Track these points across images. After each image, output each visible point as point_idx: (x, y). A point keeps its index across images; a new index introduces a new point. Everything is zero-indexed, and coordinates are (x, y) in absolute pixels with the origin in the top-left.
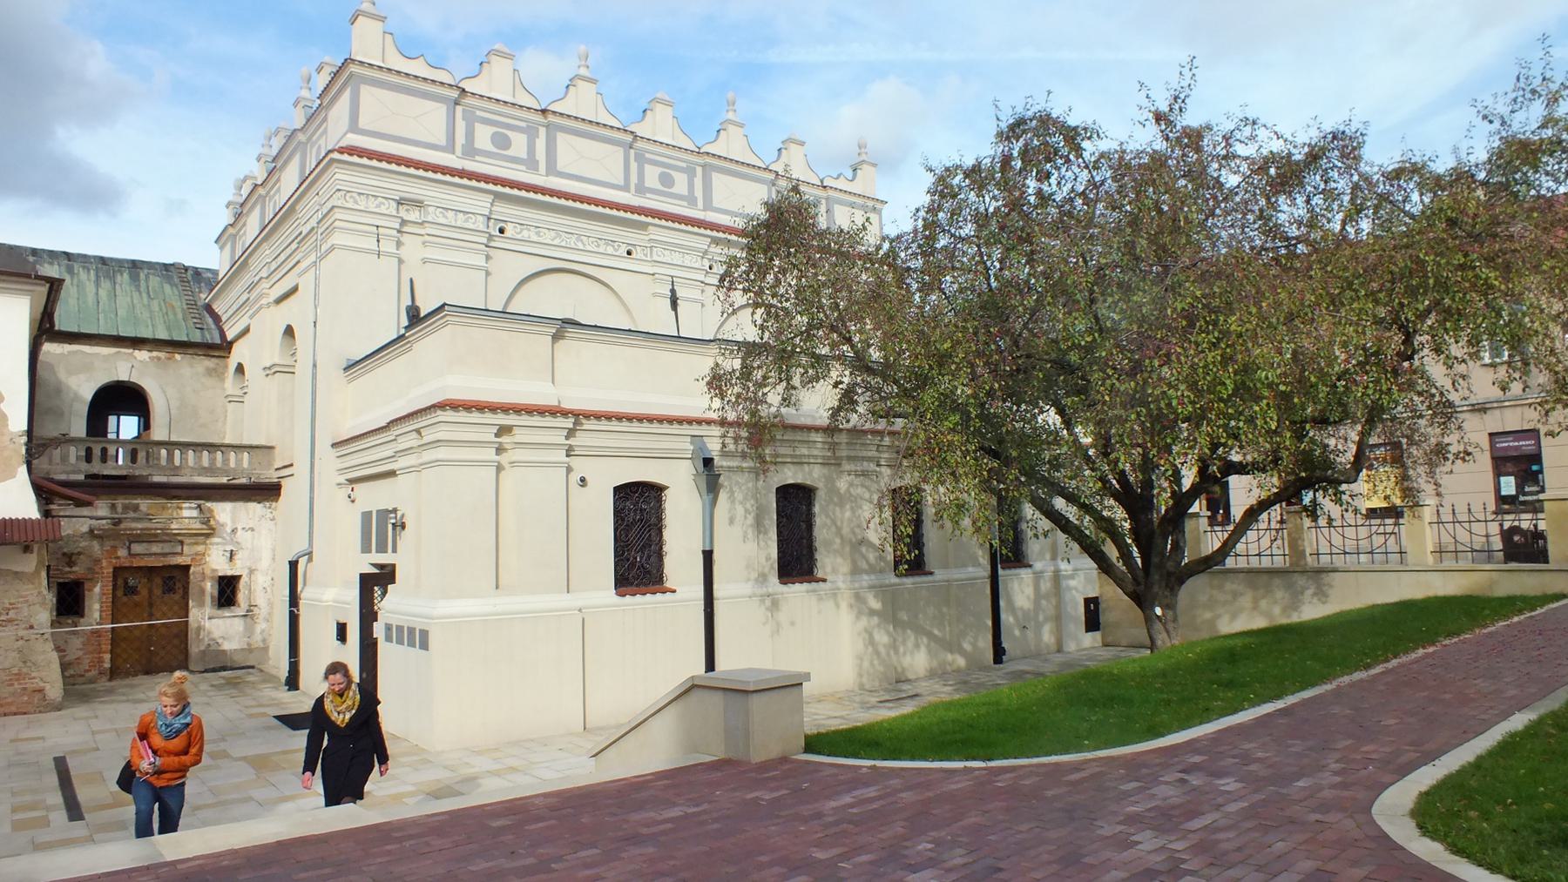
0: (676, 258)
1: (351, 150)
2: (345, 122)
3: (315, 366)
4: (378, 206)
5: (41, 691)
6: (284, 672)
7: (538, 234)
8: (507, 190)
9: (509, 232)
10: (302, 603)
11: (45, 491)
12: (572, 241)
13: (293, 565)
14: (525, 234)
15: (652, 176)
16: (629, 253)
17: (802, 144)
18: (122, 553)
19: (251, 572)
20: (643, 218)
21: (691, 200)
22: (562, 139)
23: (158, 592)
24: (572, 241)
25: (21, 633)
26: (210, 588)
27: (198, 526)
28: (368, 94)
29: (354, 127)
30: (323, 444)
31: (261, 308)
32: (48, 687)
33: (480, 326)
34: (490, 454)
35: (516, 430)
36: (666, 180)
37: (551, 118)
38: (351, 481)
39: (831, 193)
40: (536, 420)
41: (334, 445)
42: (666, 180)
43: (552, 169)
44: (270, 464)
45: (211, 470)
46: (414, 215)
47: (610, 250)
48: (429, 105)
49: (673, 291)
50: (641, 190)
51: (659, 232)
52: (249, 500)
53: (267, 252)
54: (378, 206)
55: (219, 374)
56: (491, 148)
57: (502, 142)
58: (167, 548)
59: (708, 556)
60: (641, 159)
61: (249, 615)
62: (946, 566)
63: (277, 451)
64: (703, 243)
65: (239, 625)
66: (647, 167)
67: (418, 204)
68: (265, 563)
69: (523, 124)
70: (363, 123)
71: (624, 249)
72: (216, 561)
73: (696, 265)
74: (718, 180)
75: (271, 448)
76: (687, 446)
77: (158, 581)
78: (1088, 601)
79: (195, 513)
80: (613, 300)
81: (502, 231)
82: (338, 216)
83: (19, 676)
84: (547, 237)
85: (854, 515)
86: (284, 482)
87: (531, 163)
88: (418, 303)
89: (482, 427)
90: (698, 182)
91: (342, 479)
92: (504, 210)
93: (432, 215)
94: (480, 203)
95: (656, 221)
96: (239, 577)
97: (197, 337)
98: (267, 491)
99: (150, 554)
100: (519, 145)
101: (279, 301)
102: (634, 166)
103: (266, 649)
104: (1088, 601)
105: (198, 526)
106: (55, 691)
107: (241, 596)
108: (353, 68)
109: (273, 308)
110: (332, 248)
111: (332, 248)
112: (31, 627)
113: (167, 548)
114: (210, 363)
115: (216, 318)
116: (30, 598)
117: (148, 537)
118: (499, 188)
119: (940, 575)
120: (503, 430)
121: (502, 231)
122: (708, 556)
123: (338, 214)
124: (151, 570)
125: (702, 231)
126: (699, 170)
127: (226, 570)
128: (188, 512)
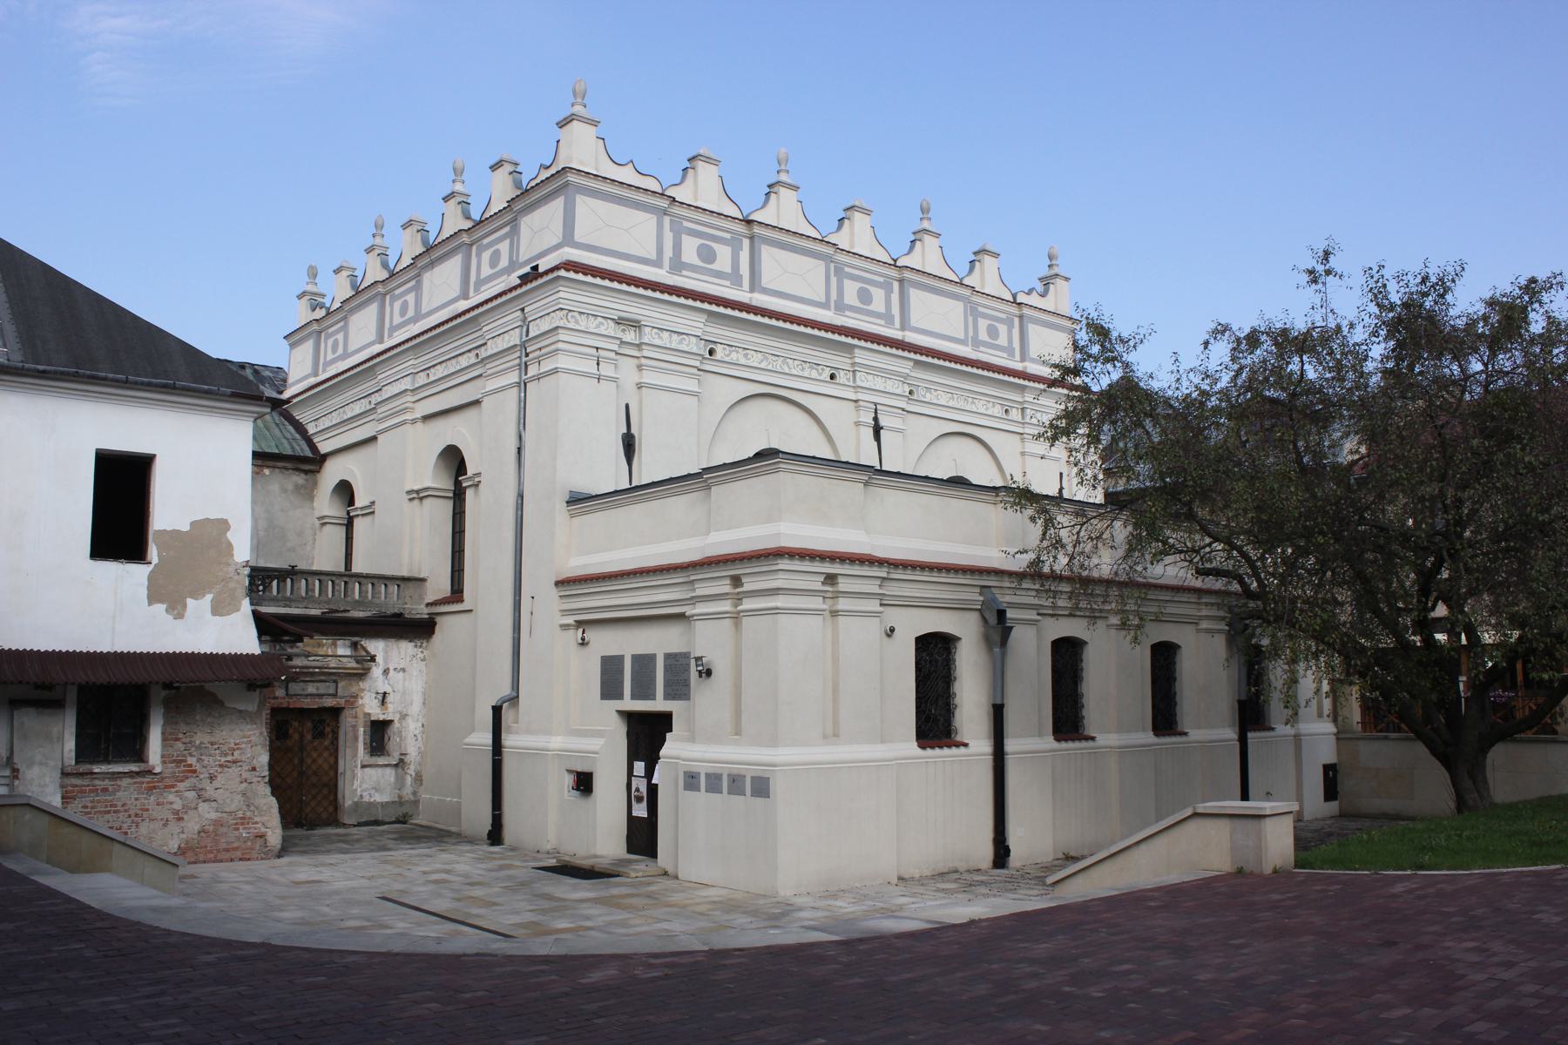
0: (879, 383)
1: (570, 266)
2: (554, 235)
3: (521, 496)
4: (598, 327)
5: (262, 836)
6: (486, 824)
8: (721, 310)
9: (719, 354)
11: (264, 625)
12: (778, 365)
13: (497, 711)
14: (734, 357)
15: (851, 290)
17: (996, 255)
19: (404, 716)
20: (849, 340)
21: (888, 318)
24: (778, 365)
25: (246, 775)
27: (354, 665)
28: (583, 204)
29: (568, 239)
30: (539, 583)
31: (403, 423)
32: (269, 833)
35: (840, 580)
36: (865, 296)
37: (757, 230)
38: (579, 623)
39: (1026, 311)
40: (909, 575)
41: (558, 583)
42: (865, 296)
44: (421, 598)
45: (360, 604)
46: (630, 336)
47: (814, 374)
49: (876, 419)
50: (841, 307)
51: (865, 355)
53: (410, 363)
54: (598, 327)
56: (697, 262)
57: (707, 255)
60: (839, 272)
61: (401, 764)
63: (428, 584)
64: (905, 367)
65: (390, 774)
66: (847, 282)
67: (636, 325)
68: (416, 708)
69: (728, 236)
70: (579, 236)
71: (828, 372)
72: (370, 706)
73: (898, 391)
74: (915, 295)
75: (423, 580)
76: (975, 596)
78: (1327, 768)
79: (348, 652)
80: (815, 428)
81: (711, 352)
82: (562, 337)
83: (244, 821)
84: (755, 359)
85: (1114, 672)
86: (438, 619)
88: (634, 431)
89: (808, 576)
90: (895, 297)
91: (570, 620)
93: (649, 336)
94: (693, 322)
95: (862, 343)
96: (391, 722)
98: (421, 629)
99: (311, 694)
100: (723, 260)
102: (834, 280)
103: (416, 803)
104: (1327, 768)
105: (354, 665)
106: (275, 836)
107: (393, 744)
108: (571, 178)
109: (419, 425)
110: (555, 371)
111: (555, 371)
112: (254, 769)
113: (323, 688)
114: (299, 479)
115: (300, 428)
117: (305, 675)
118: (714, 308)
120: (831, 579)
121: (711, 352)
123: (563, 336)
125: (906, 354)
127: (377, 713)
128: (343, 649)
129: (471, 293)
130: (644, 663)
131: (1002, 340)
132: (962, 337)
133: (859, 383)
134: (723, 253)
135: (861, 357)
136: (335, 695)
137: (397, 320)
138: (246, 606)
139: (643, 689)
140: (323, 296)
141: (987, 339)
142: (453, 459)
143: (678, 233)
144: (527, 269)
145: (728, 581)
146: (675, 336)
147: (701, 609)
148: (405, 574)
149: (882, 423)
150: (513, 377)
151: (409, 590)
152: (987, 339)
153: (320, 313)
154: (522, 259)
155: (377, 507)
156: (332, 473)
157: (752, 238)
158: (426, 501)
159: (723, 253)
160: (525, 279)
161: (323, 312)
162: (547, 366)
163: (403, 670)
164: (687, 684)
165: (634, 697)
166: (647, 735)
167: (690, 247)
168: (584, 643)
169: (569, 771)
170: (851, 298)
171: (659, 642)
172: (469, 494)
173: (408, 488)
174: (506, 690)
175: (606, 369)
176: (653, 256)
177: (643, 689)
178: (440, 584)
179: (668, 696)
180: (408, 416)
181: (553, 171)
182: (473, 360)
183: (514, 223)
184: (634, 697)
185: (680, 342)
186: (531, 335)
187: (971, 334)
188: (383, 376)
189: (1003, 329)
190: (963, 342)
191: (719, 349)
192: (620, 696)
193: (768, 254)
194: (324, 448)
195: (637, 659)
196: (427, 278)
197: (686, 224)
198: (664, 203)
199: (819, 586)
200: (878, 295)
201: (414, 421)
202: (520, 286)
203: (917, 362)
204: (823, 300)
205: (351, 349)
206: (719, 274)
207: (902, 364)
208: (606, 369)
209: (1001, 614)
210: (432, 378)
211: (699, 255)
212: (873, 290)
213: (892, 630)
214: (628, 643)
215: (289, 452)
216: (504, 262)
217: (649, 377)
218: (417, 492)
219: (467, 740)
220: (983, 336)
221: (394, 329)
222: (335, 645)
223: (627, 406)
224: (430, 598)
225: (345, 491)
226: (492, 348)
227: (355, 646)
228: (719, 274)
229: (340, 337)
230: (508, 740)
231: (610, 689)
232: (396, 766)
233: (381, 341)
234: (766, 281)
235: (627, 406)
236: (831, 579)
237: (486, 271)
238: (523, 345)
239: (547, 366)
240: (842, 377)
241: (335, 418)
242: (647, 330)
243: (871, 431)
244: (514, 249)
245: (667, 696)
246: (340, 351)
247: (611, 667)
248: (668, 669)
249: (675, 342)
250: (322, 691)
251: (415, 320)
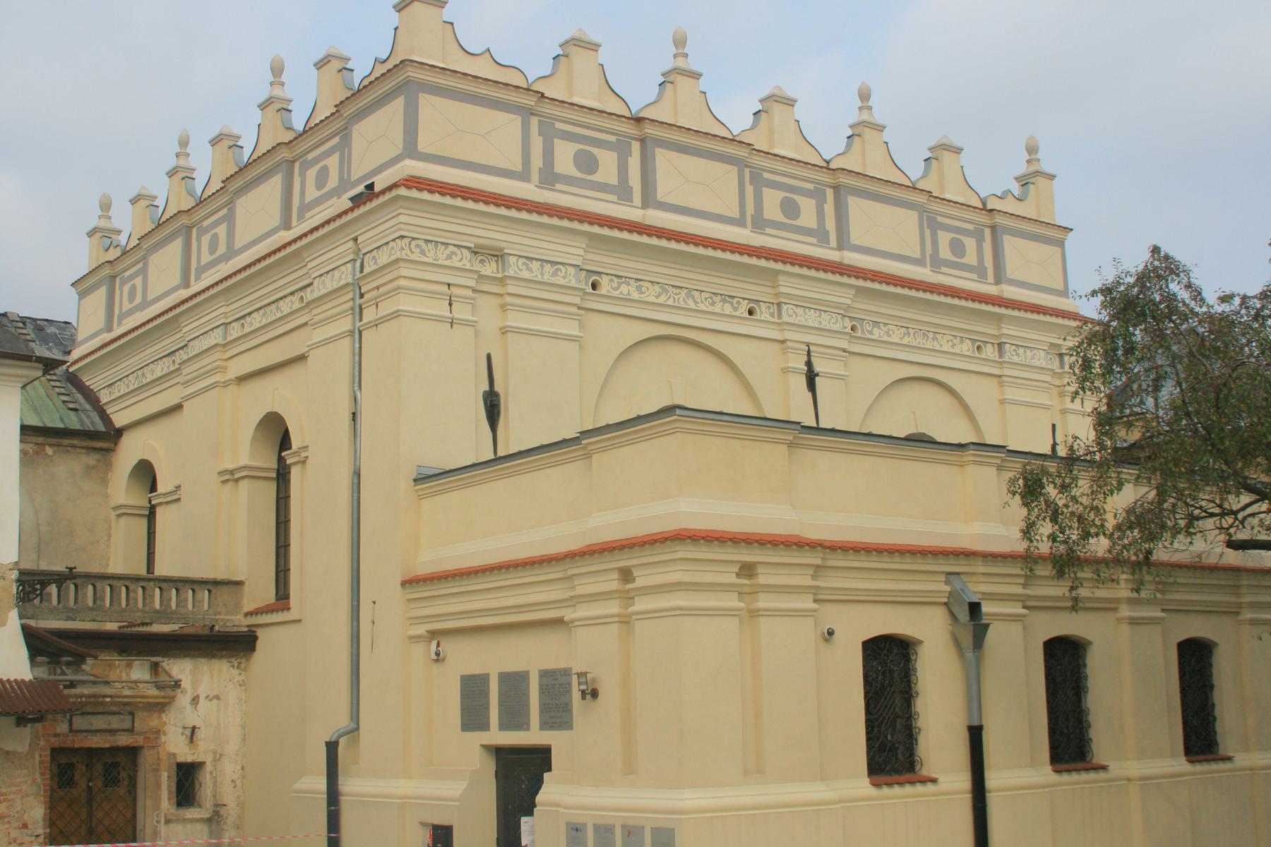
1: (413, 182)
2: (395, 144)
3: (357, 474)
7: (639, 288)
8: (606, 231)
9: (605, 288)
10: (343, 800)
11: (39, 644)
13: (332, 748)
15: (772, 202)
16: (751, 312)
18: (63, 727)
20: (771, 265)
21: (820, 235)
22: (853, 203)
23: (99, 783)
26: (166, 781)
28: (428, 104)
29: (411, 149)
33: (704, 433)
35: (760, 570)
36: (790, 208)
37: (649, 130)
38: (433, 634)
42: (790, 208)
43: (649, 200)
44: (238, 606)
45: (164, 615)
46: (490, 269)
48: (501, 117)
49: (809, 364)
50: (760, 223)
51: (792, 284)
52: (214, 657)
53: (220, 311)
55: (103, 471)
56: (574, 172)
57: (587, 163)
58: (115, 722)
59: (976, 735)
60: (757, 179)
62: (1247, 749)
63: (246, 588)
64: (843, 297)
66: (766, 191)
67: (499, 256)
68: (232, 747)
70: (424, 145)
71: (744, 306)
72: (176, 746)
73: (837, 327)
75: (239, 584)
77: (99, 767)
82: (404, 272)
84: (651, 294)
86: (260, 633)
87: (623, 192)
88: (498, 388)
89: (719, 567)
90: (829, 209)
91: (421, 630)
92: (602, 260)
93: (514, 267)
94: (570, 250)
95: (788, 268)
97: (73, 422)
98: (238, 644)
99: (97, 733)
101: (243, 379)
102: (749, 190)
108: (412, 73)
110: (397, 314)
111: (397, 314)
112: (25, 826)
113: (115, 722)
114: (91, 459)
115: (91, 397)
116: (24, 787)
117: (95, 707)
118: (596, 229)
119: (1241, 759)
121: (594, 286)
122: (976, 735)
124: (91, 753)
125: (845, 280)
126: (830, 193)
127: (185, 754)
128: (139, 671)
129: (294, 222)
130: (514, 683)
131: (970, 258)
132: (917, 255)
133: (786, 318)
134: (608, 162)
135: (788, 286)
136: (131, 731)
137: (206, 258)
138: (14, 620)
139: (514, 717)
140: (119, 232)
141: (950, 257)
142: (277, 432)
143: (549, 134)
144: (360, 188)
145: (615, 575)
146: (547, 267)
147: (582, 612)
148: (220, 576)
149: (818, 367)
150: (345, 324)
151: (222, 595)
152: (950, 257)
153: (113, 254)
154: (354, 177)
155: (183, 494)
156: (130, 451)
157: (642, 141)
158: (244, 484)
159: (608, 162)
160: (358, 201)
161: (118, 252)
162: (386, 308)
163: (217, 697)
164: (567, 708)
165: (504, 726)
166: (520, 774)
167: (565, 155)
168: (439, 658)
169: (423, 824)
170: (772, 211)
171: (531, 656)
172: (295, 473)
173: (222, 468)
174: (342, 720)
175: (461, 312)
176: (518, 167)
177: (514, 717)
178: (261, 590)
179: (546, 725)
180: (217, 378)
181: (390, 65)
182: (297, 305)
183: (345, 133)
184: (504, 726)
185: (555, 274)
186: (367, 270)
187: (929, 250)
188: (189, 328)
189: (970, 243)
190: (919, 262)
191: (604, 281)
192: (484, 726)
193: (664, 160)
194: (119, 420)
195: (505, 678)
196: (242, 204)
197: (558, 125)
198: (530, 101)
199: (732, 579)
200: (807, 207)
201: (226, 384)
202: (352, 209)
203: (859, 290)
204: (736, 215)
205: (150, 297)
206: (603, 187)
207: (839, 293)
208: (461, 312)
209: (974, 608)
210: (248, 329)
212: (800, 199)
213: (831, 633)
214: (493, 658)
215: (78, 427)
216: (333, 181)
217: (515, 320)
218: (232, 472)
219: (297, 786)
220: (945, 253)
221: (202, 270)
222: (129, 666)
223: (489, 357)
224: (246, 609)
225: (146, 473)
226: (319, 289)
227: (155, 667)
228: (603, 187)
229: (138, 281)
230: (348, 785)
231: (473, 718)
232: (209, 820)
233: (186, 285)
234: (662, 194)
235: (489, 357)
236: (747, 570)
237: (312, 193)
238: (357, 284)
239: (386, 308)
240: (763, 313)
241: (133, 383)
242: (512, 260)
243: (803, 380)
244: (345, 164)
245: (546, 725)
246: (138, 300)
247: (473, 688)
248: (543, 689)
249: (547, 274)
250: (115, 726)
251: (227, 257)
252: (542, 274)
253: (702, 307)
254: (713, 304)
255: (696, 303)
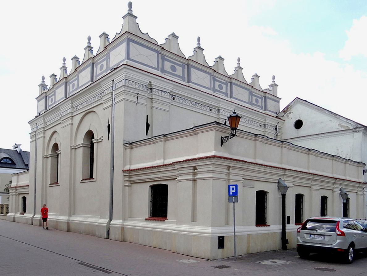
34: (191, 177)
88: (149, 123)
146: (163, 92)
185: (164, 95)
211: (171, 68)
223: (147, 116)
235: (147, 116)
242: (154, 90)
252: (161, 94)
253: (198, 107)
254: (201, 107)
255: (198, 107)
